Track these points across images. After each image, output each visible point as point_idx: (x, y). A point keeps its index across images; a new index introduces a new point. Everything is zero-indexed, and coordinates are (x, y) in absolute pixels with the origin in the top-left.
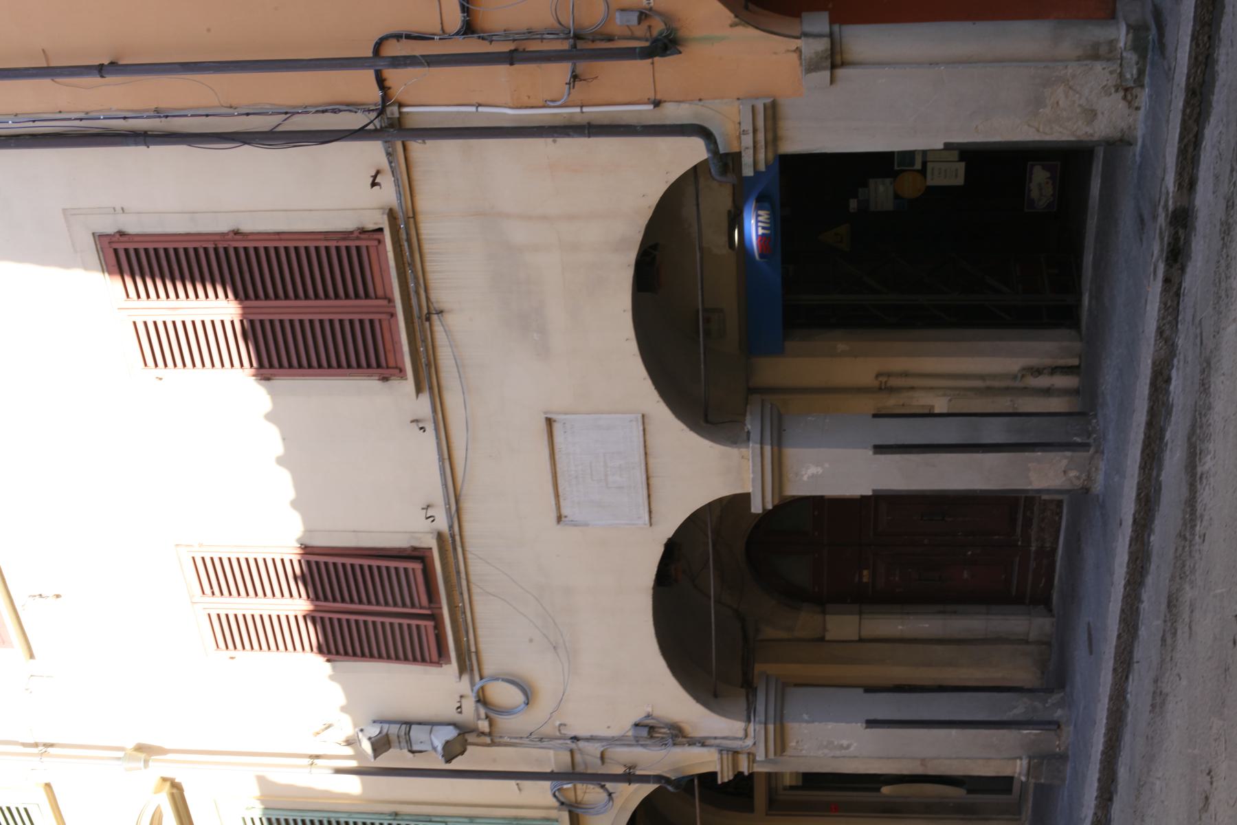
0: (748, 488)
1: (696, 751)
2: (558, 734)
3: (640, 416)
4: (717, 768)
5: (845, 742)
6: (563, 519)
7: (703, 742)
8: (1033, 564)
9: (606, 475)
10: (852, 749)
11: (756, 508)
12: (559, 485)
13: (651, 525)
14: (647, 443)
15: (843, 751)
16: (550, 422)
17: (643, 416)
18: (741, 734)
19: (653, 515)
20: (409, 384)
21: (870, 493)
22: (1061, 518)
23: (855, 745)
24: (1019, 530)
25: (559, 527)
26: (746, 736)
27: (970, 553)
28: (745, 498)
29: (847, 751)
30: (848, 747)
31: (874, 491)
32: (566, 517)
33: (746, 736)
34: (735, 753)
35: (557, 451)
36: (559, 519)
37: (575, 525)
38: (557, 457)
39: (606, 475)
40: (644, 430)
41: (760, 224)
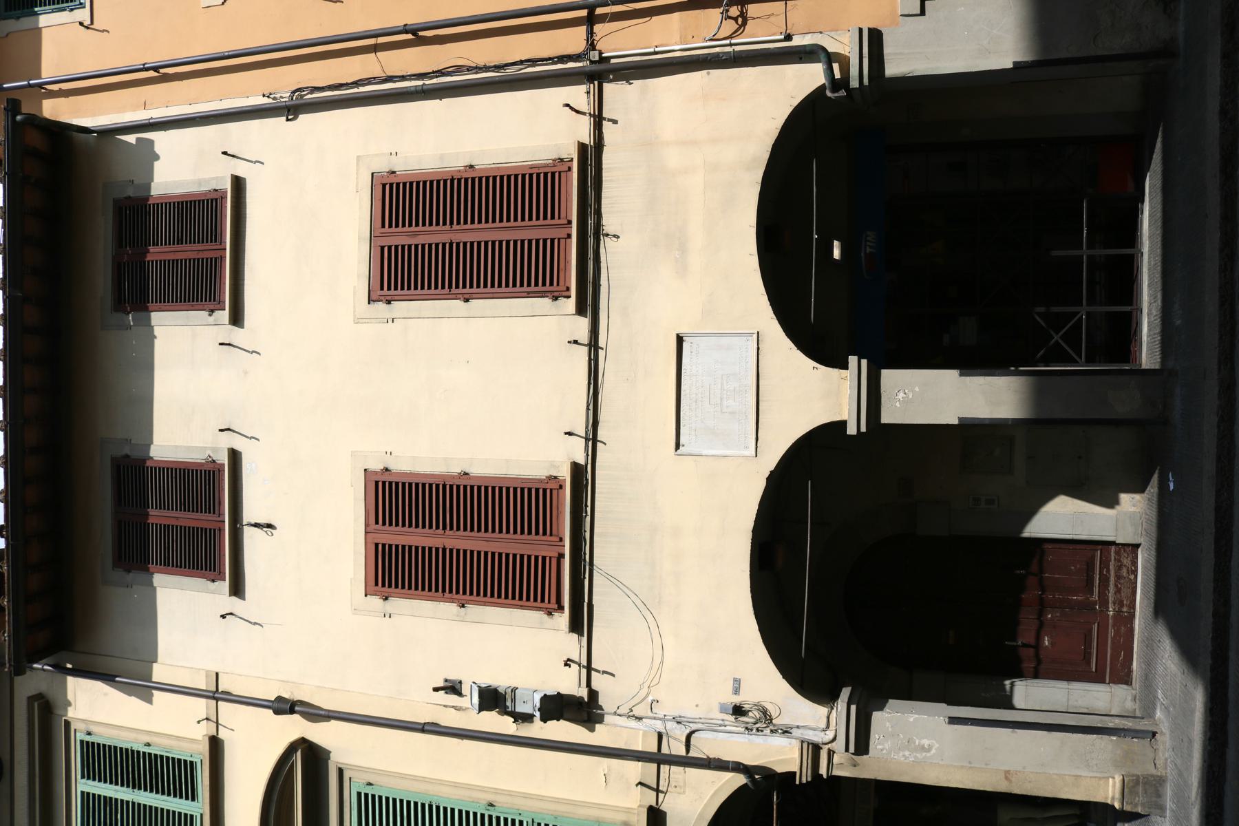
0: (844, 416)
1: (779, 741)
2: (650, 714)
4: (796, 768)
5: (926, 742)
6: (681, 447)
7: (786, 732)
8: (1111, 632)
9: (722, 399)
10: (933, 751)
11: (852, 430)
15: (924, 754)
16: (680, 340)
18: (823, 725)
20: (572, 301)
21: (956, 422)
22: (1136, 577)
23: (937, 745)
24: (1096, 590)
26: (828, 726)
27: (1050, 616)
28: (842, 424)
29: (928, 755)
30: (929, 750)
31: (960, 419)
33: (828, 726)
34: (816, 748)
36: (678, 446)
39: (722, 399)
40: (758, 349)
41: (868, 243)
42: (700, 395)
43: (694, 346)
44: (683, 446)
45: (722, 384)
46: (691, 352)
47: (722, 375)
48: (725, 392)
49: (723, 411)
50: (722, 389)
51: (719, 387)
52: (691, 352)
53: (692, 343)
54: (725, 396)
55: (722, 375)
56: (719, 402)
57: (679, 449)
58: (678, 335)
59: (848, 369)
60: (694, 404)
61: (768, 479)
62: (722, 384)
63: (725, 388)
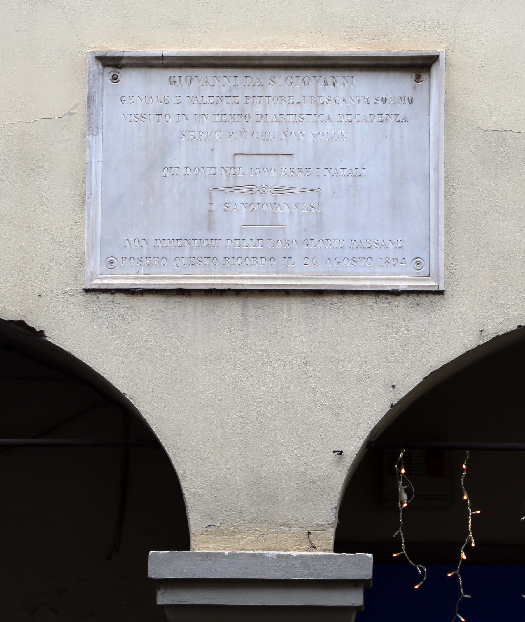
3: (441, 289)
9: (249, 189)
12: (220, 73)
13: (87, 291)
14: (346, 299)
17: (440, 293)
19: (120, 298)
25: (91, 59)
32: (115, 79)
35: (328, 75)
37: (90, 99)
38: (308, 74)
39: (249, 189)
40: (395, 293)
42: (260, 127)
43: (404, 109)
44: (115, 79)
45: (292, 190)
46: (384, 100)
47: (318, 190)
48: (270, 198)
49: (215, 194)
50: (278, 191)
51: (285, 182)
52: (384, 100)
53: (411, 100)
54: (258, 199)
55: (318, 190)
56: (241, 182)
57: (105, 66)
58: (435, 59)
59: (336, 551)
60: (236, 109)
61: (21, 324)
62: (292, 190)
63: (283, 199)
